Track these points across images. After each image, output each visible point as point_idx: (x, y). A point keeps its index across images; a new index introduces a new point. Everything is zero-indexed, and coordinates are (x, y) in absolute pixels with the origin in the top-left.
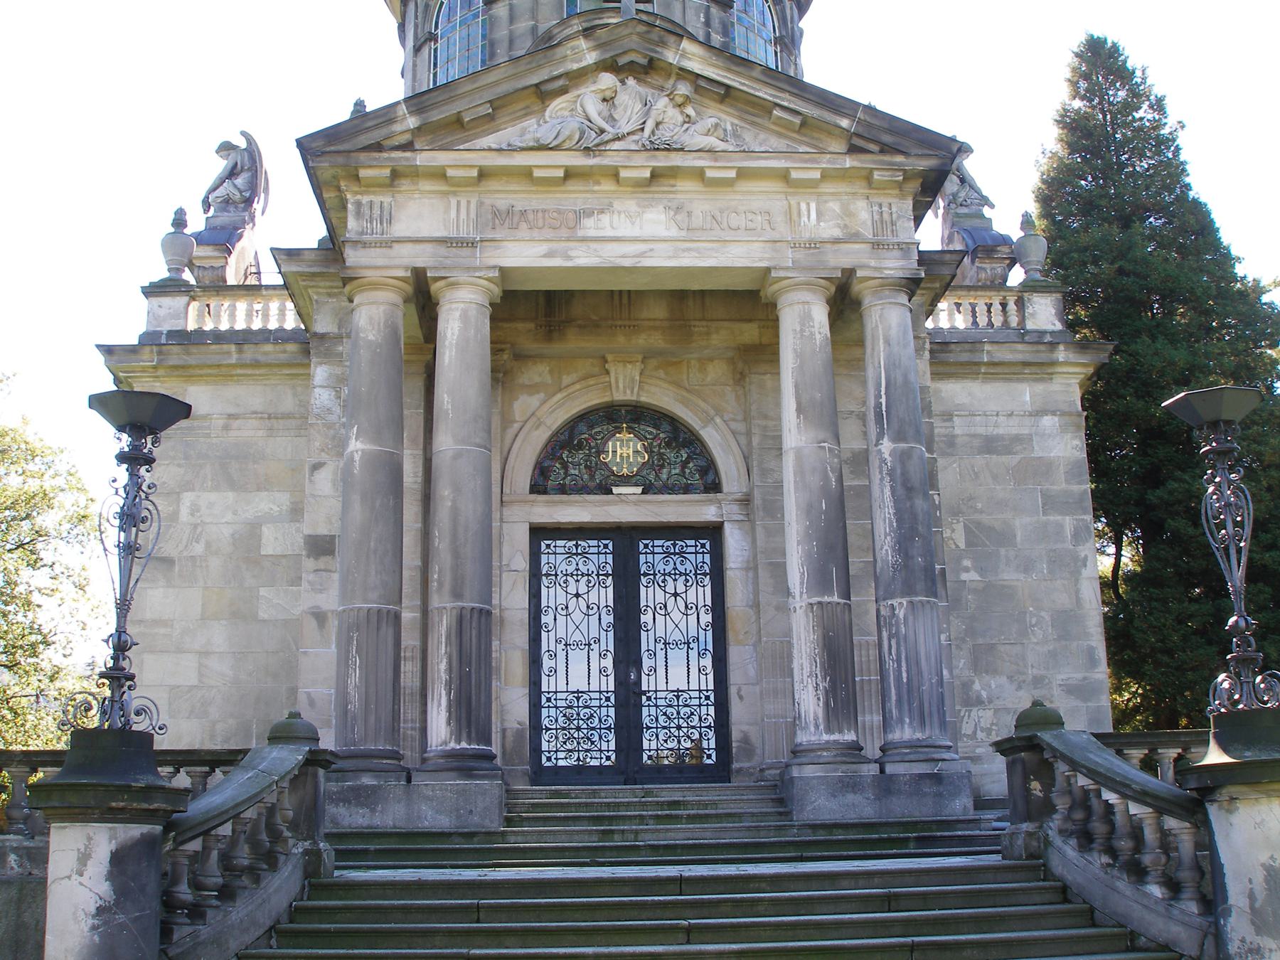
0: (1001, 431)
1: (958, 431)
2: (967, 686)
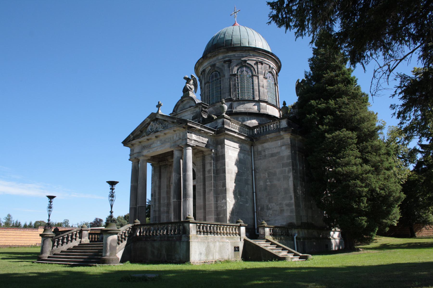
0: (274, 152)
1: (266, 154)
2: (267, 206)
